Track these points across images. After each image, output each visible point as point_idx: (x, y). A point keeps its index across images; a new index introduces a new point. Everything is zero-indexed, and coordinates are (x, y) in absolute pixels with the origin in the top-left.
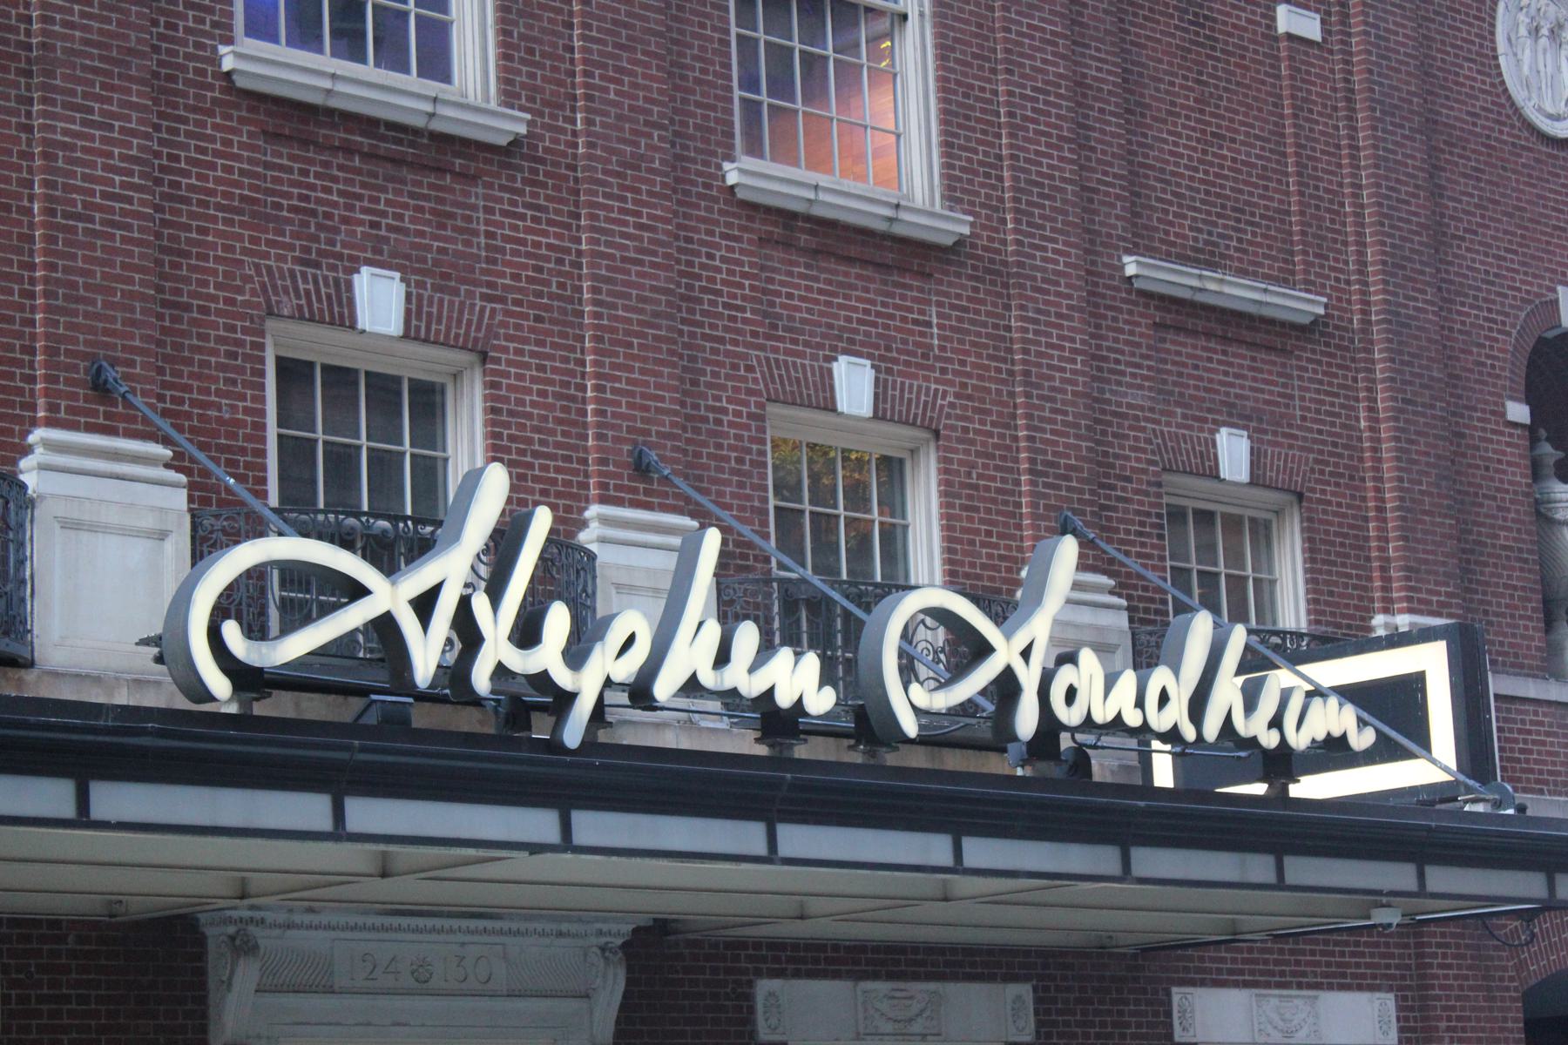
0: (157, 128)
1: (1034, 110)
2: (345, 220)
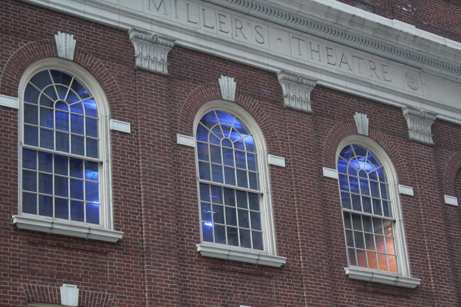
0: (180, 269)
1: (436, 246)
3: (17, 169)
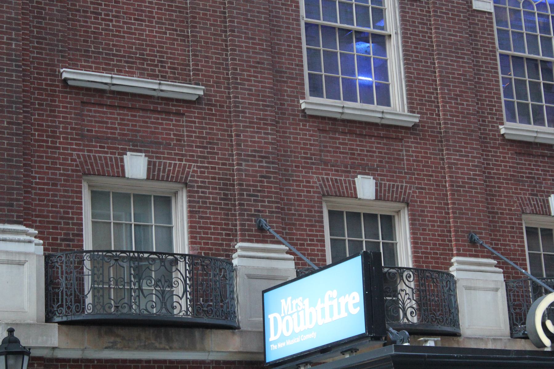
0: (482, 155)
2: (544, 179)
3: (301, 48)
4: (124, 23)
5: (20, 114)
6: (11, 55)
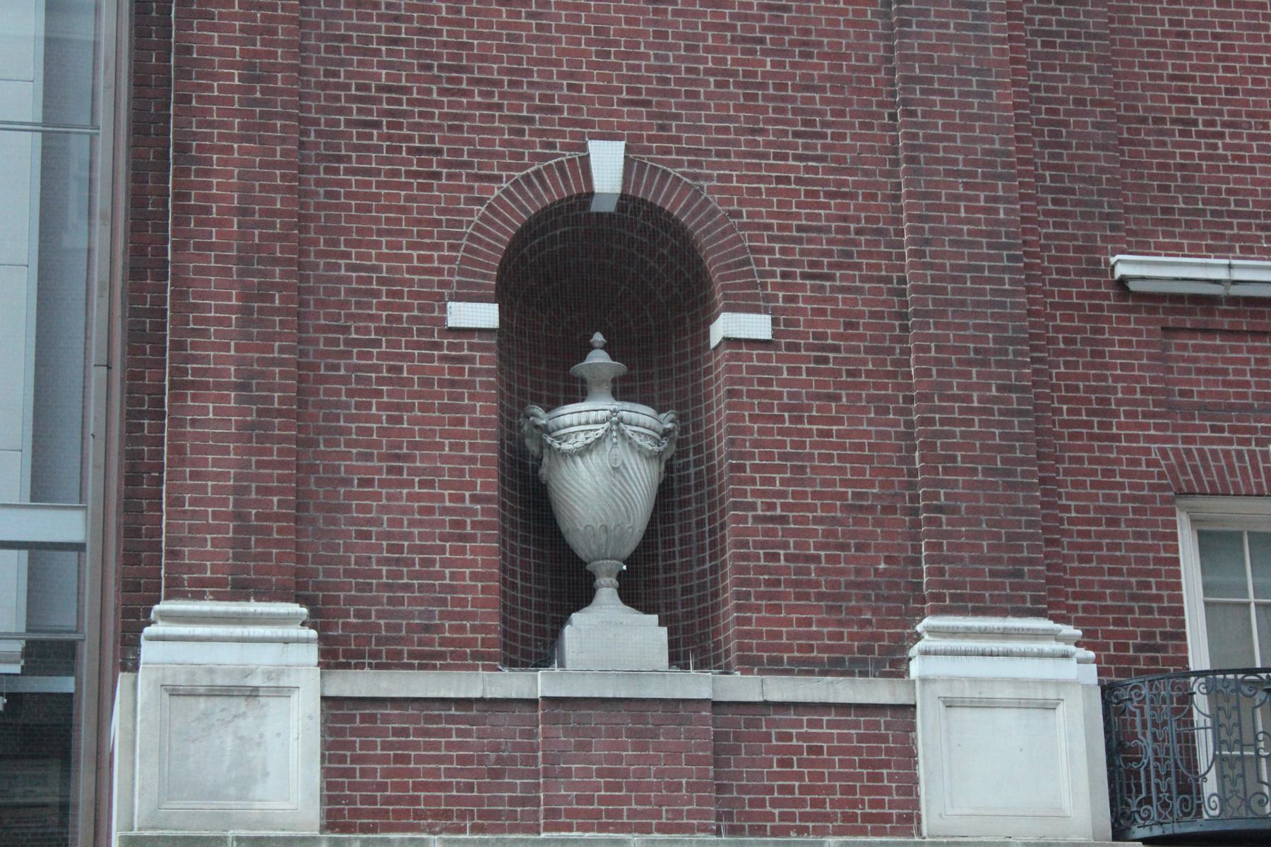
4: (1252, 137)
5: (1025, 365)
6: (997, 235)
